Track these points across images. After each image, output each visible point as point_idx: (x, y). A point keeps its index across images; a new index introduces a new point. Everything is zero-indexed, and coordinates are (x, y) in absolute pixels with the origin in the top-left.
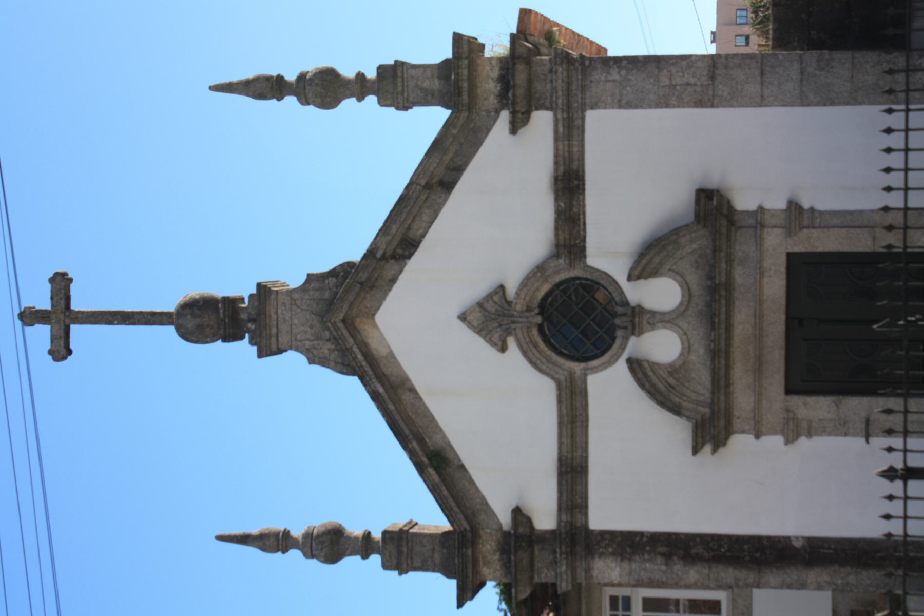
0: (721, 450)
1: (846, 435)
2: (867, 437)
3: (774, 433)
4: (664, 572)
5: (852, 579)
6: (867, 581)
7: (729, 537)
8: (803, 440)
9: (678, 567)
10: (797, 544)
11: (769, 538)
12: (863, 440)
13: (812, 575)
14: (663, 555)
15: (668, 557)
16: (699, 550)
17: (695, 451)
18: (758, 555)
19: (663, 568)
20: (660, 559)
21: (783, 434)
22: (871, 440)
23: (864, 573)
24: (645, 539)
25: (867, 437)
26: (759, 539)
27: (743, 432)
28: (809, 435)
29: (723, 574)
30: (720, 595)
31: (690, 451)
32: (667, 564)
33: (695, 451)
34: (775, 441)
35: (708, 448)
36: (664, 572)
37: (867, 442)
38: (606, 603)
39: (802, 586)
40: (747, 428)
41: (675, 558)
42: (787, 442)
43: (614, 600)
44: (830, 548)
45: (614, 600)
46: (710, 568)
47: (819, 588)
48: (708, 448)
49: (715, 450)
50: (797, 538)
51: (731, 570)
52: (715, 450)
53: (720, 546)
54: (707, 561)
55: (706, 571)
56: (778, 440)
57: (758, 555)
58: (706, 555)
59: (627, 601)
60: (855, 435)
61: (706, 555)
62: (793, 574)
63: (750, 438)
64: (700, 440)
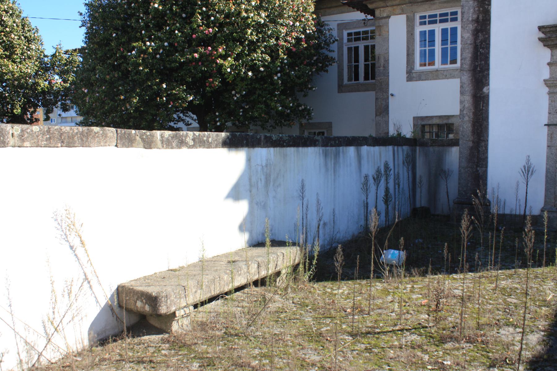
0: (541, 44)
1: (549, 113)
2: (548, 125)
3: (551, 74)
4: (468, 20)
5: (467, 118)
6: (465, 127)
7: (488, 53)
8: (547, 90)
9: (471, 27)
10: (485, 90)
11: (488, 74)
12: (547, 123)
13: (468, 98)
14: (478, 18)
15: (477, 21)
16: (481, 37)
17: (540, 28)
18: (479, 69)
19: (470, 19)
20: (475, 16)
21: (550, 78)
22: (546, 127)
23: (470, 125)
24: (486, 7)
25: (548, 125)
26: (488, 69)
27: (552, 55)
28: (549, 93)
29: (467, 51)
30: (458, 64)
31: (541, 24)
32: (472, 21)
33: (540, 28)
34: (546, 74)
35: (542, 35)
36: (468, 20)
37: (545, 125)
38: (454, 10)
39: (462, 93)
40: (555, 57)
41: (476, 25)
42: (544, 80)
43: (456, 13)
44: (483, 107)
45: (456, 13)
46: (471, 44)
47: (461, 102)
48: (542, 35)
49: (540, 39)
50: (489, 89)
51: (470, 55)
52: (540, 39)
53: (483, 48)
54: (475, 42)
55: (469, 42)
56: (547, 76)
57: (479, 69)
58: (478, 41)
59: (455, 19)
60: (549, 118)
61: (478, 41)
62: (469, 88)
63: (548, 60)
64: (548, 30)
